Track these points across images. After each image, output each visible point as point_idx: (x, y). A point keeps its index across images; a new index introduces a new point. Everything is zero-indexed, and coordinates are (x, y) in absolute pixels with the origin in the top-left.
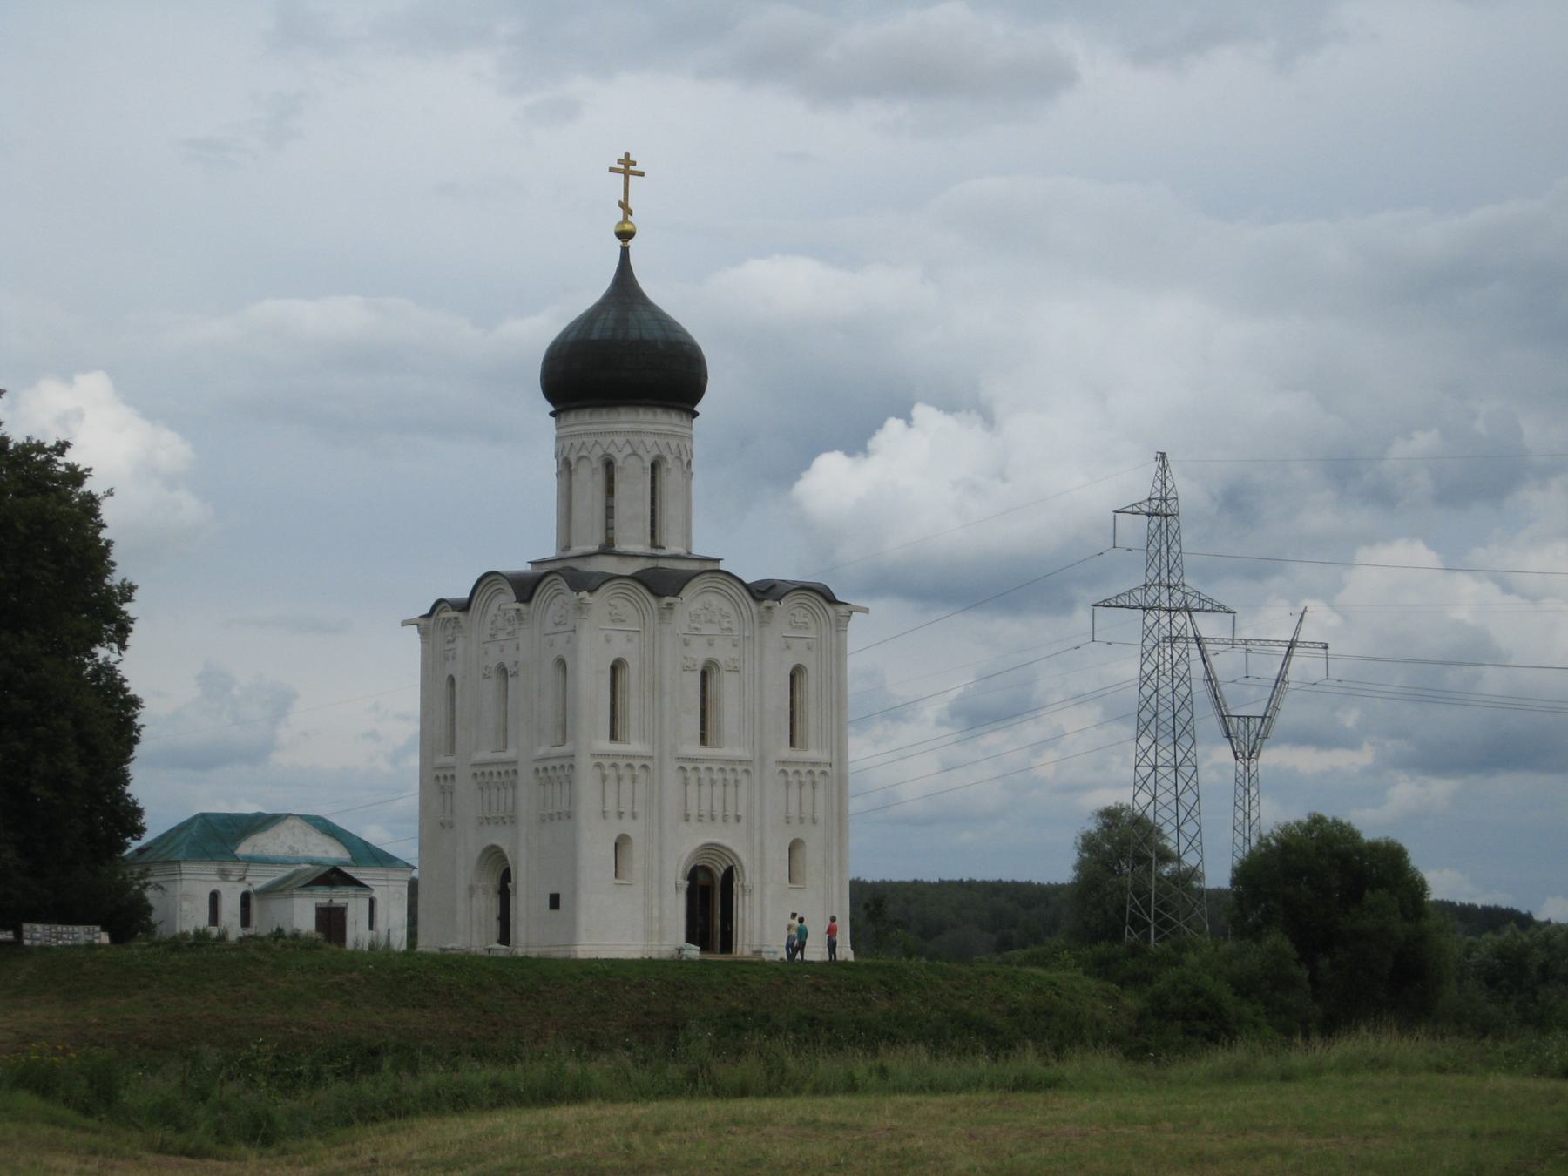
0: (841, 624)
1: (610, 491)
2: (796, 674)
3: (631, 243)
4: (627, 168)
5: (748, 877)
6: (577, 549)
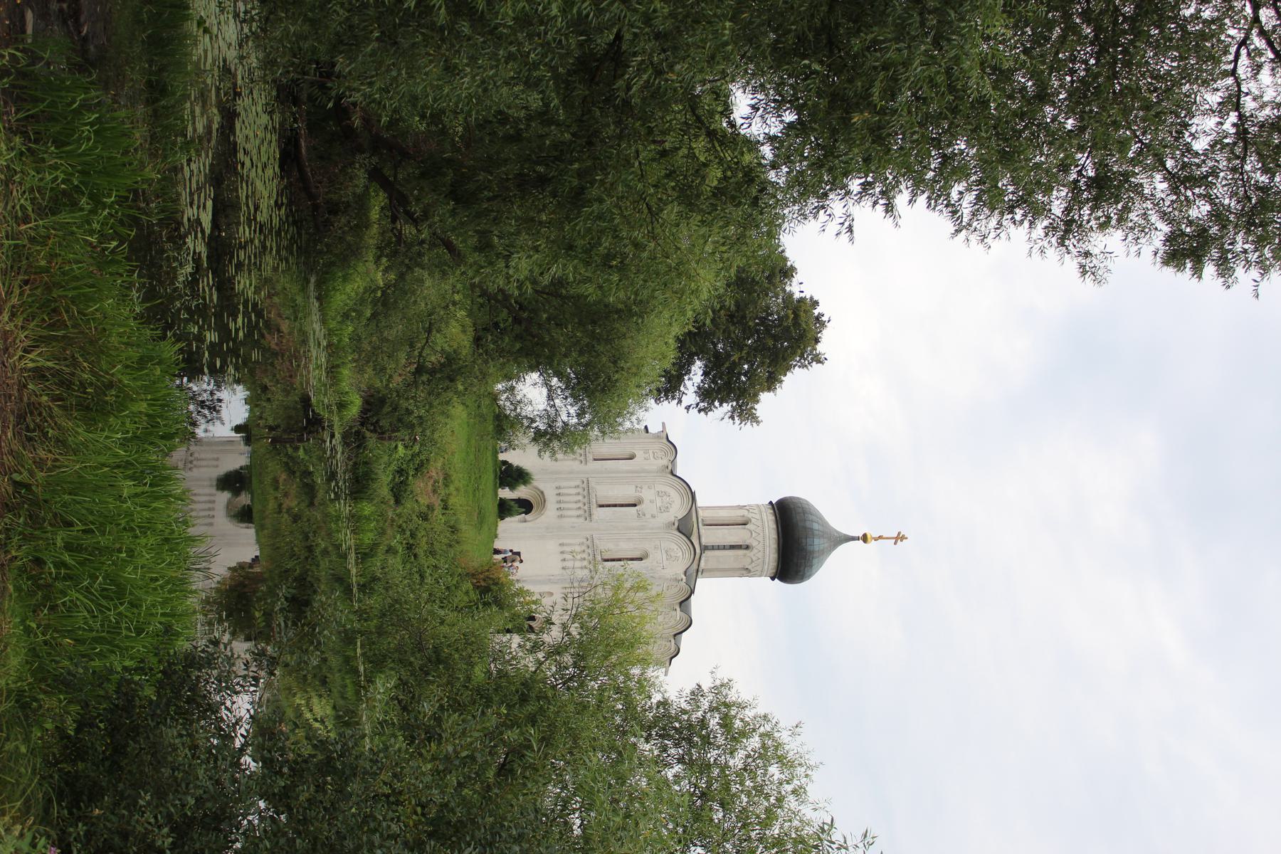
1: (732, 547)
4: (900, 538)
6: (702, 531)
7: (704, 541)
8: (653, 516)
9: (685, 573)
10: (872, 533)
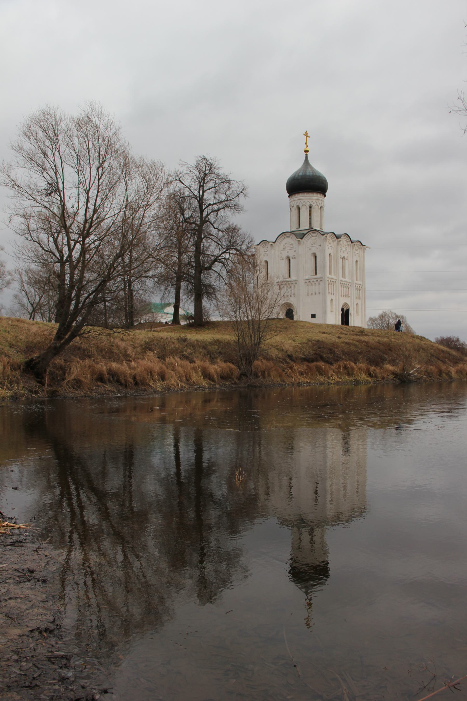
0: (364, 251)
1: (310, 214)
2: (356, 261)
3: (308, 153)
4: (306, 134)
5: (351, 312)
6: (302, 228)
7: (308, 228)
8: (295, 251)
9: (323, 235)
10: (304, 147)
